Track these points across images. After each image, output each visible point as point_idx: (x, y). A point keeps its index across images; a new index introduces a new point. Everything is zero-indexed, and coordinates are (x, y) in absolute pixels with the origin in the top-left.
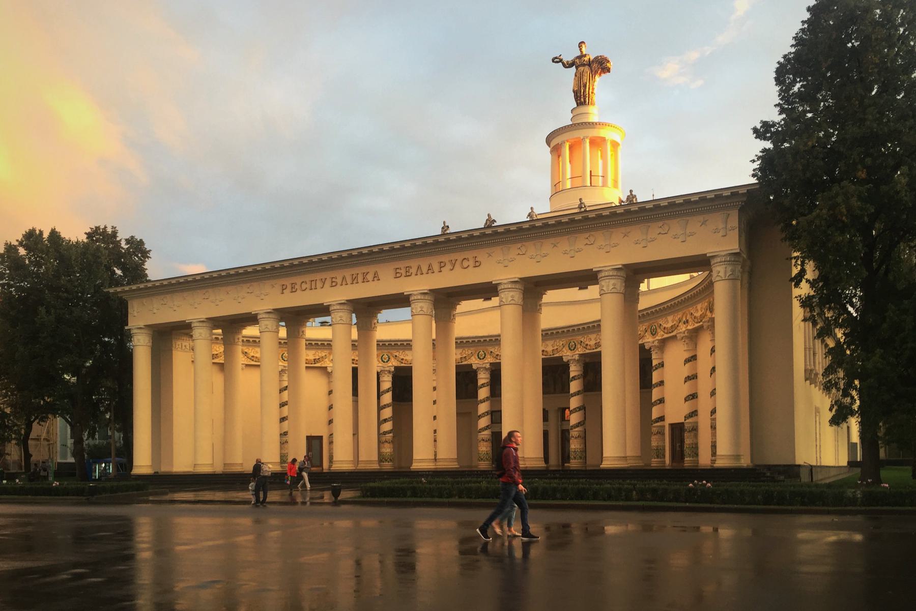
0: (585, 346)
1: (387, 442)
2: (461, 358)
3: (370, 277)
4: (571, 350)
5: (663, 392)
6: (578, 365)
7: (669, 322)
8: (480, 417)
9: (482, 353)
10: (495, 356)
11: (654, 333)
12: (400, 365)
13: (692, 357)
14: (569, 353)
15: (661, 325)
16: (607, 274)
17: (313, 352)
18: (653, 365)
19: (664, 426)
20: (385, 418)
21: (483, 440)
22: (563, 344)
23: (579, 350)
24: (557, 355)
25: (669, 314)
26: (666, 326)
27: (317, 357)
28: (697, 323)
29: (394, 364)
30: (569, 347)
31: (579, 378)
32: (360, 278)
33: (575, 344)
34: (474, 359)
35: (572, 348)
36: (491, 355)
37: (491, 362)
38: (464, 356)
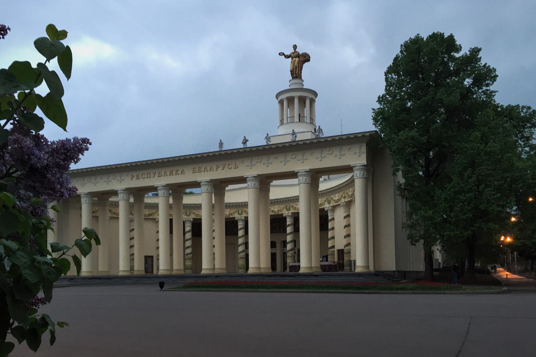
0: (294, 208)
1: (189, 259)
3: (179, 172)
4: (287, 210)
5: (334, 233)
6: (291, 218)
7: (336, 197)
8: (239, 246)
9: (240, 211)
11: (329, 202)
12: (196, 218)
13: (348, 215)
14: (286, 212)
15: (332, 198)
16: (302, 174)
17: (148, 210)
18: (329, 219)
19: (334, 251)
20: (188, 246)
21: (241, 258)
22: (283, 207)
23: (292, 210)
24: (280, 213)
25: (337, 193)
26: (335, 199)
27: (151, 213)
28: (350, 198)
29: (193, 217)
30: (286, 209)
31: (291, 225)
32: (174, 173)
33: (289, 207)
34: (236, 215)
35: (288, 210)
38: (231, 213)
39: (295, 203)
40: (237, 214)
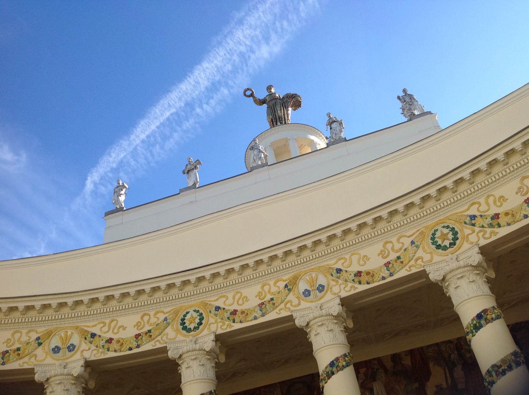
2: (137, 336)
14: (438, 256)
22: (412, 243)
23: (473, 238)
24: (402, 273)
30: (434, 243)
33: (453, 229)
36: (216, 315)
37: (220, 331)
38: (147, 328)
39: (482, 200)
40: (177, 330)
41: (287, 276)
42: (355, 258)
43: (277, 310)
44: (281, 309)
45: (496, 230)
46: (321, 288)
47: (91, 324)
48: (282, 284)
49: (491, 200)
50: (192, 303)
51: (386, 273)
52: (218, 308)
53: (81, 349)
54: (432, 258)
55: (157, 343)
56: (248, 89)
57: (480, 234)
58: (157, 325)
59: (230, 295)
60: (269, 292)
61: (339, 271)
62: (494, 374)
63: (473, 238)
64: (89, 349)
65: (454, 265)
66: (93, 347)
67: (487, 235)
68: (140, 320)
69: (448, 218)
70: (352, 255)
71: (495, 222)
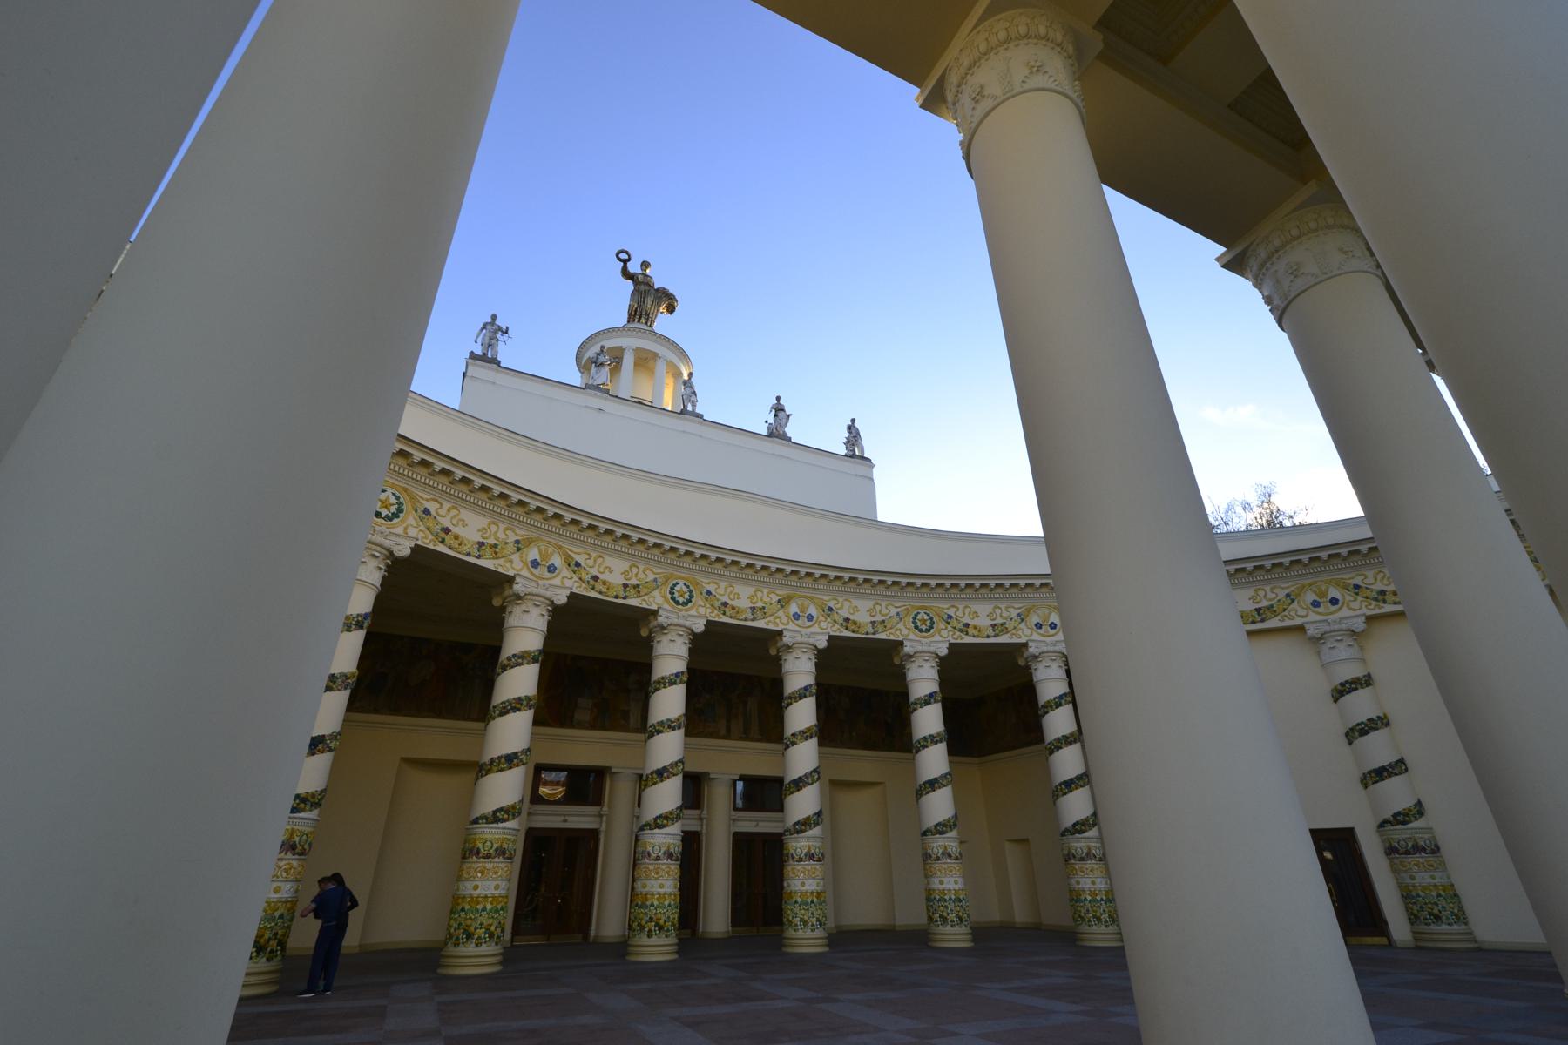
10: (718, 604)
12: (431, 546)
22: (898, 614)
23: (944, 633)
33: (931, 619)
36: (706, 599)
38: (634, 582)
39: (961, 607)
41: (783, 593)
42: (847, 604)
43: (766, 620)
44: (769, 622)
45: (963, 636)
46: (810, 618)
47: (574, 549)
48: (775, 598)
49: (967, 610)
50: (683, 575)
51: (870, 630)
52: (709, 593)
53: (562, 575)
54: (908, 635)
55: (644, 603)
56: (627, 253)
57: (951, 633)
58: (647, 582)
59: (723, 585)
60: (761, 600)
61: (831, 609)
62: (929, 740)
63: (944, 633)
64: (571, 578)
65: (925, 648)
66: (575, 579)
67: (955, 636)
68: (628, 569)
69: (931, 608)
70: (846, 600)
71: (965, 629)
